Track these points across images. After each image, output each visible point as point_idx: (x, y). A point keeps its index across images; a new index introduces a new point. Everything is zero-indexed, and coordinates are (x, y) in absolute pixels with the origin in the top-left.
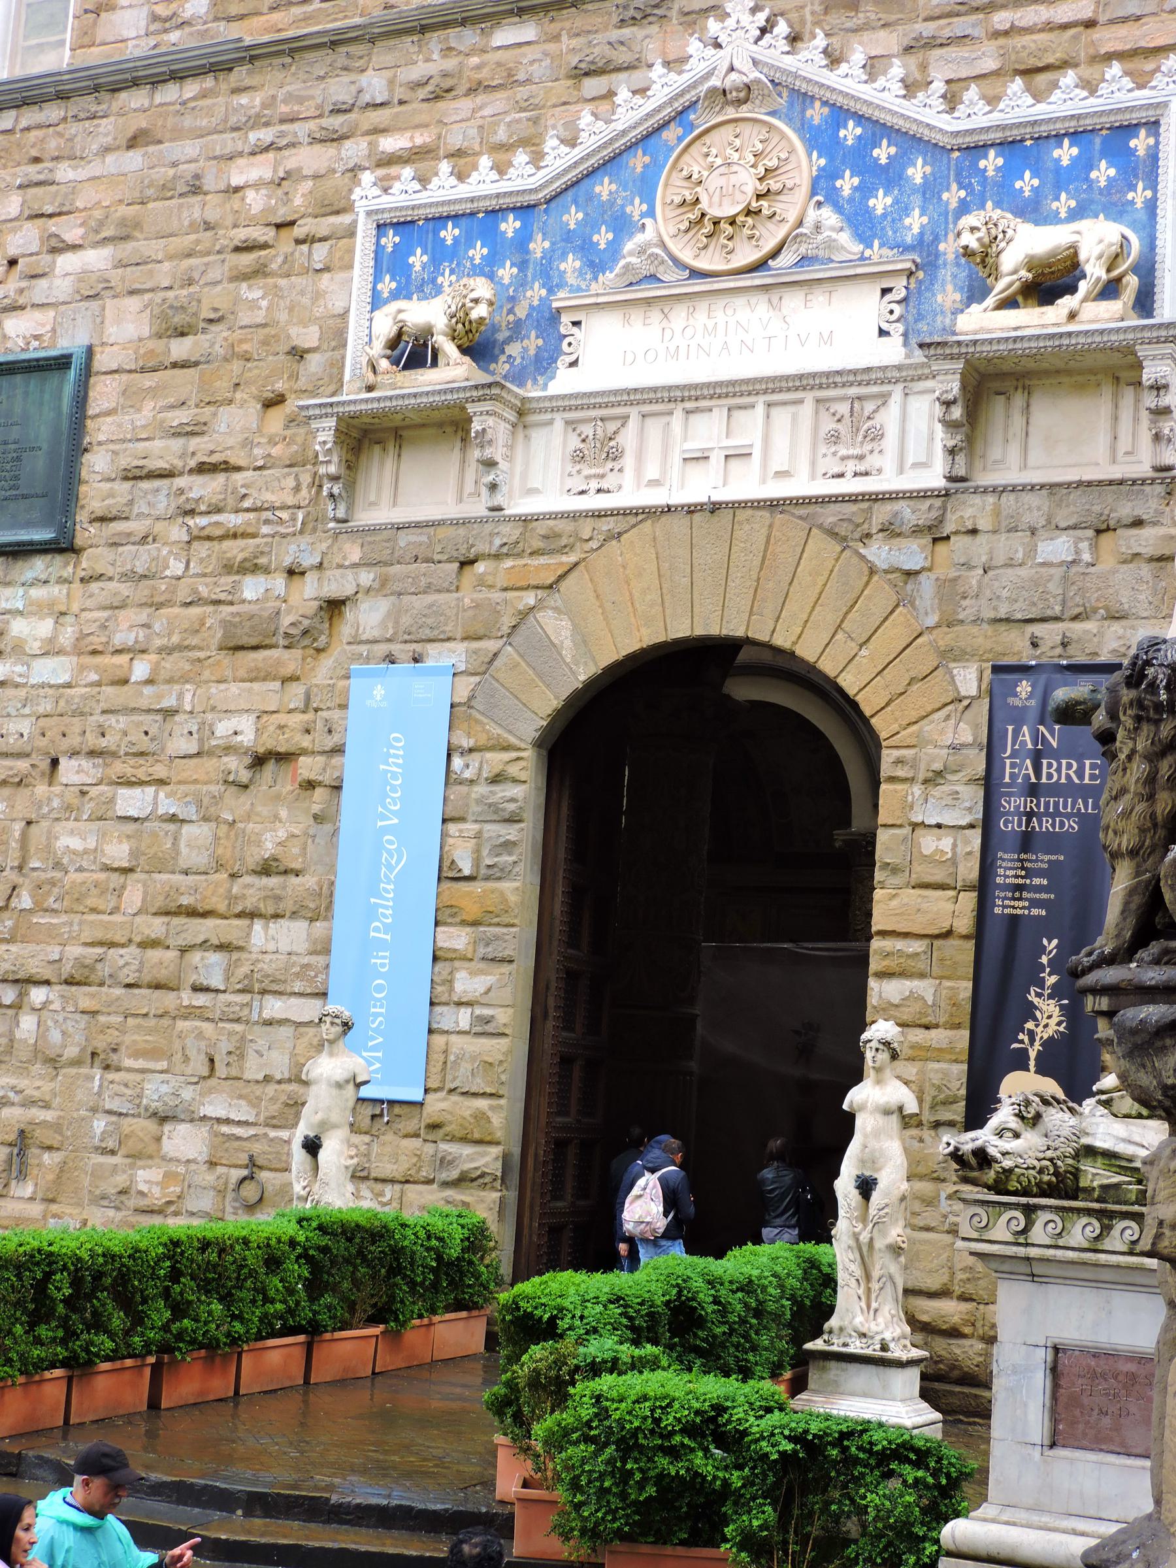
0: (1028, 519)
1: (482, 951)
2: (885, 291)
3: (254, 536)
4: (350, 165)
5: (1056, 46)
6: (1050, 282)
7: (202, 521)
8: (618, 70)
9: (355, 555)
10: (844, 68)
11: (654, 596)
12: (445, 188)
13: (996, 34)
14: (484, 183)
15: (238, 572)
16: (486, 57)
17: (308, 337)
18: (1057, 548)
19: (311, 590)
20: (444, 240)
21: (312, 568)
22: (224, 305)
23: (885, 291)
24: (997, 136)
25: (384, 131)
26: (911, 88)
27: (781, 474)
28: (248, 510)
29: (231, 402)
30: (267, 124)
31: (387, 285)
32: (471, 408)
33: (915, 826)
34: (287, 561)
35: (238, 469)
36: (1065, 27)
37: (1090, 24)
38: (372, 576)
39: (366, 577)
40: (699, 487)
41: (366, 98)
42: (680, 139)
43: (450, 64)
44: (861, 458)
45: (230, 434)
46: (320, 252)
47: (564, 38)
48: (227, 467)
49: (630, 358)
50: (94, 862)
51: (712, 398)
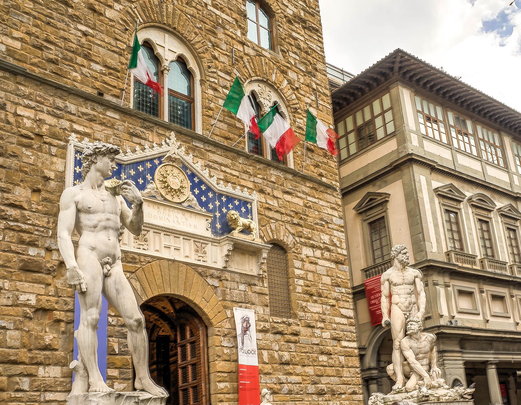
0: (237, 280)
2: (207, 220)
3: (32, 233)
5: (234, 179)
6: (247, 230)
7: (12, 224)
8: (142, 138)
11: (161, 281)
13: (222, 171)
15: (26, 245)
16: (106, 117)
17: (52, 175)
18: (242, 287)
22: (18, 152)
23: (207, 220)
25: (74, 122)
26: (211, 176)
27: (187, 257)
28: (29, 224)
29: (18, 185)
30: (31, 100)
34: (47, 245)
35: (25, 209)
37: (238, 177)
41: (69, 110)
43: (96, 113)
45: (20, 196)
46: (54, 150)
48: (21, 208)
49: (150, 216)
51: (171, 233)
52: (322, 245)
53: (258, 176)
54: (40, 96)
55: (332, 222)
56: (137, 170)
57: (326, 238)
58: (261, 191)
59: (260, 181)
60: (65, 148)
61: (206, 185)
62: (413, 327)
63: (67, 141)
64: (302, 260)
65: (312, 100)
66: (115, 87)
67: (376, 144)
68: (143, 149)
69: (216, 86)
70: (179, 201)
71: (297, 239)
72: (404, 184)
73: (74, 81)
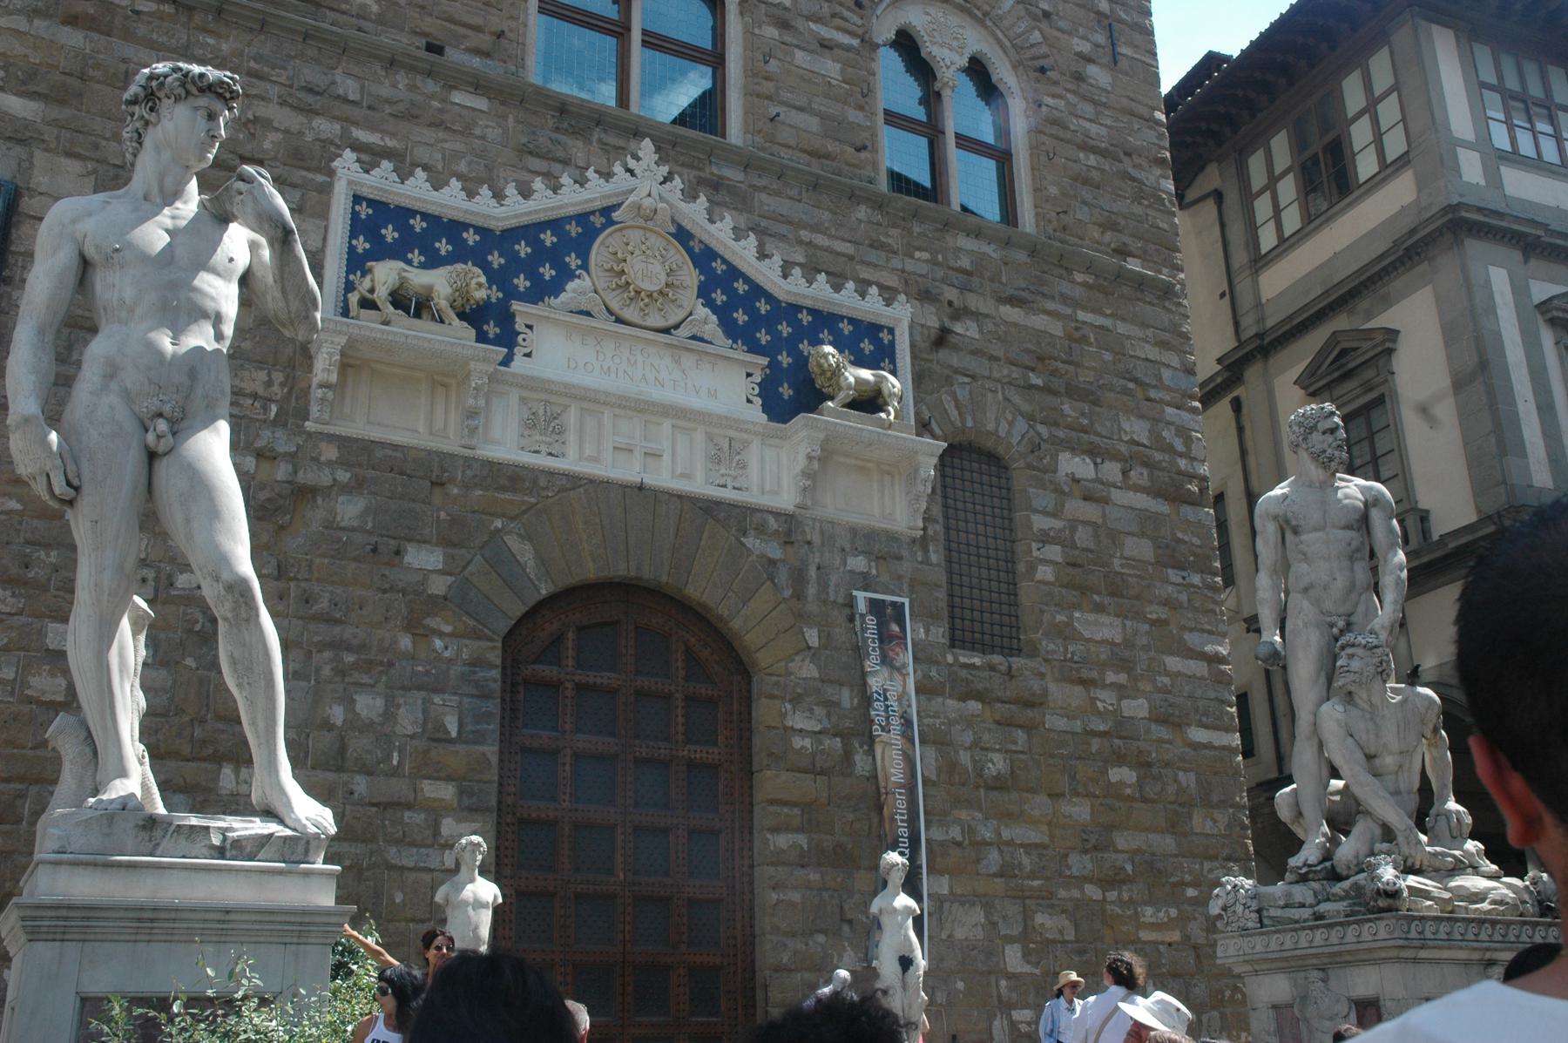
1: (466, 802)
2: (749, 375)
4: (324, 136)
6: (869, 402)
9: (330, 453)
10: (719, 224)
12: (416, 191)
13: (801, 242)
14: (451, 200)
19: (282, 471)
20: (413, 227)
21: (286, 454)
23: (749, 375)
24: (809, 303)
25: (356, 124)
26: (763, 255)
27: (683, 475)
31: (362, 244)
32: (472, 365)
33: (786, 728)
34: (259, 444)
36: (839, 254)
37: (851, 258)
38: (348, 475)
39: (343, 476)
40: (628, 471)
41: (341, 91)
42: (604, 227)
44: (735, 478)
47: (511, 119)
49: (573, 364)
50: (12, 694)
52: (1123, 448)
53: (917, 254)
54: (258, 58)
55: (1160, 384)
56: (536, 243)
57: (1137, 429)
58: (925, 296)
59: (924, 269)
60: (326, 190)
61: (747, 280)
62: (1355, 665)
63: (331, 173)
64: (1058, 490)
65: (1097, 46)
66: (478, 29)
67: (1354, 196)
68: (556, 189)
69: (787, 15)
70: (662, 323)
71: (1042, 429)
72: (1438, 298)
73: (359, 17)
